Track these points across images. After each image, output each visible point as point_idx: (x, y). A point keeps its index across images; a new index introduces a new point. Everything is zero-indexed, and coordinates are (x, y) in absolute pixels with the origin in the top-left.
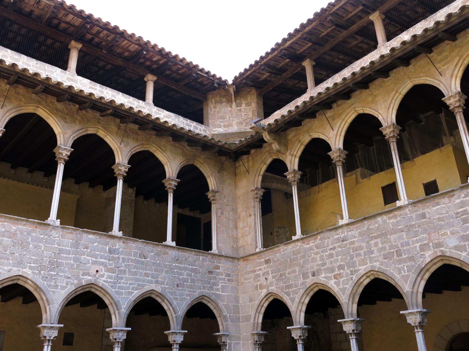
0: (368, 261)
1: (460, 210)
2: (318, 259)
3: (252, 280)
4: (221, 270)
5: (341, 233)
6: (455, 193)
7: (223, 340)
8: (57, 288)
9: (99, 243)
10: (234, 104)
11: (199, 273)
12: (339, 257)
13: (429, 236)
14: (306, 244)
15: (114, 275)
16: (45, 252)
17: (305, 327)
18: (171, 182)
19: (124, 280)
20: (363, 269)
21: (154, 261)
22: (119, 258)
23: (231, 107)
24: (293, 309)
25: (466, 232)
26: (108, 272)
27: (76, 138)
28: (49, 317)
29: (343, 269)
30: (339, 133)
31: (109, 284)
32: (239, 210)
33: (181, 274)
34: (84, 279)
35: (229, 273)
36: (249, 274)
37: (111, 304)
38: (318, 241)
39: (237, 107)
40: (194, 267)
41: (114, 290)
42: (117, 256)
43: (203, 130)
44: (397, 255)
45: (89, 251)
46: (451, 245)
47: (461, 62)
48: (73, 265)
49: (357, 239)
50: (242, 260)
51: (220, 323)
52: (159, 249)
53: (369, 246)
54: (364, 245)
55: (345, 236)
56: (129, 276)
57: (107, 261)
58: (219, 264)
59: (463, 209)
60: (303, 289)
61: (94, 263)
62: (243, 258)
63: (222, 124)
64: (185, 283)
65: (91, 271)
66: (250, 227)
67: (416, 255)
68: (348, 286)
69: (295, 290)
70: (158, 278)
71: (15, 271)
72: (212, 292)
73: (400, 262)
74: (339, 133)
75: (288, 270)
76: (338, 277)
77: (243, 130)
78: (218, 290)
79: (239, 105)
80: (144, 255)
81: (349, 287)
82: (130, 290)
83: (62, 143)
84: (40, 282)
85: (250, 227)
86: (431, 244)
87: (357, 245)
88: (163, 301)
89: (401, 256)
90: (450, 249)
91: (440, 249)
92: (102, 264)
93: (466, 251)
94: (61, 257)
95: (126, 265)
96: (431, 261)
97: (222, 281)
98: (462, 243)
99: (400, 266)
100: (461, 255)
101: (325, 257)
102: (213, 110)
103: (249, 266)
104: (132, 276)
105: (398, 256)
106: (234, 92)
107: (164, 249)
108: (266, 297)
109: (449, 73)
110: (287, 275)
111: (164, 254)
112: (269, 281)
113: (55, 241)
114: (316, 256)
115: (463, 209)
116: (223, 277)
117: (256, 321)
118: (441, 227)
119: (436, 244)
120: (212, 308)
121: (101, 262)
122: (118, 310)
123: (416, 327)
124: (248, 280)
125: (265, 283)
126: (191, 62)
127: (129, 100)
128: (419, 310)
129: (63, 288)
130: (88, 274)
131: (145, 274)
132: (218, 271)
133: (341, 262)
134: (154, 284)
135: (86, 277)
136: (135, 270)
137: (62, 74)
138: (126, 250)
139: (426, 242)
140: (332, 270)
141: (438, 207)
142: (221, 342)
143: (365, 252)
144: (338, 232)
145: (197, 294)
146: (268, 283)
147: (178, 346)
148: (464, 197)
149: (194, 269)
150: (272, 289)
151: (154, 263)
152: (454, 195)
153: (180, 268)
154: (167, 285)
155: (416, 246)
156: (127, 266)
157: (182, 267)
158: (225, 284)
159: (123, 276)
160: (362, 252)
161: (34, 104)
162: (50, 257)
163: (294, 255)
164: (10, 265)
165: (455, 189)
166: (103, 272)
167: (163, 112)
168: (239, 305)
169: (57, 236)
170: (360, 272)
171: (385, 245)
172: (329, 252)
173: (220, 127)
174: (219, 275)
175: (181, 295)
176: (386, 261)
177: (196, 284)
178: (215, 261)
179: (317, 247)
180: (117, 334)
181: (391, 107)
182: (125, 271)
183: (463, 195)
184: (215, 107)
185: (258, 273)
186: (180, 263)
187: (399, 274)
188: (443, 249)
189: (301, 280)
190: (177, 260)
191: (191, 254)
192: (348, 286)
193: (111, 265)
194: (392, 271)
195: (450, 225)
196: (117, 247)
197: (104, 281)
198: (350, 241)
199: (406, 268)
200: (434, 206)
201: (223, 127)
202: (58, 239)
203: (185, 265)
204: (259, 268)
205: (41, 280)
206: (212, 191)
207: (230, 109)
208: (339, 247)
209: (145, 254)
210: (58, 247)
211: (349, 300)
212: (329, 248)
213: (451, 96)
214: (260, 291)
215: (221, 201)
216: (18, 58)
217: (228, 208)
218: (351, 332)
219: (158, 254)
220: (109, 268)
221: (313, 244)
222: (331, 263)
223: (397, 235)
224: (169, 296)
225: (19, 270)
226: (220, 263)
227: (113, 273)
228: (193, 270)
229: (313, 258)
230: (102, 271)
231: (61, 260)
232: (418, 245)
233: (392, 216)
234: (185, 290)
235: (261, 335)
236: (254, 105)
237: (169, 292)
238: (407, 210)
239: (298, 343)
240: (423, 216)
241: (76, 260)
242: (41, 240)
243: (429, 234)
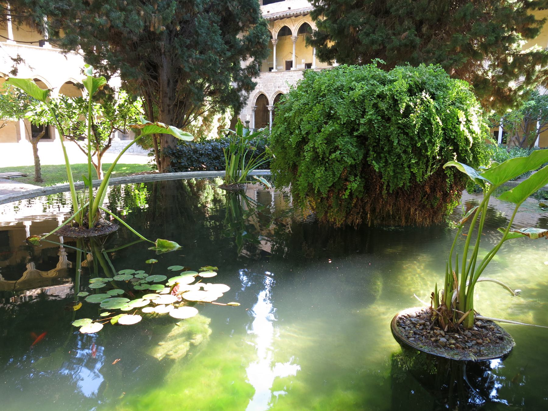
38: (282, 75)
112: (260, 87)
179: (281, 77)
189: (274, 89)
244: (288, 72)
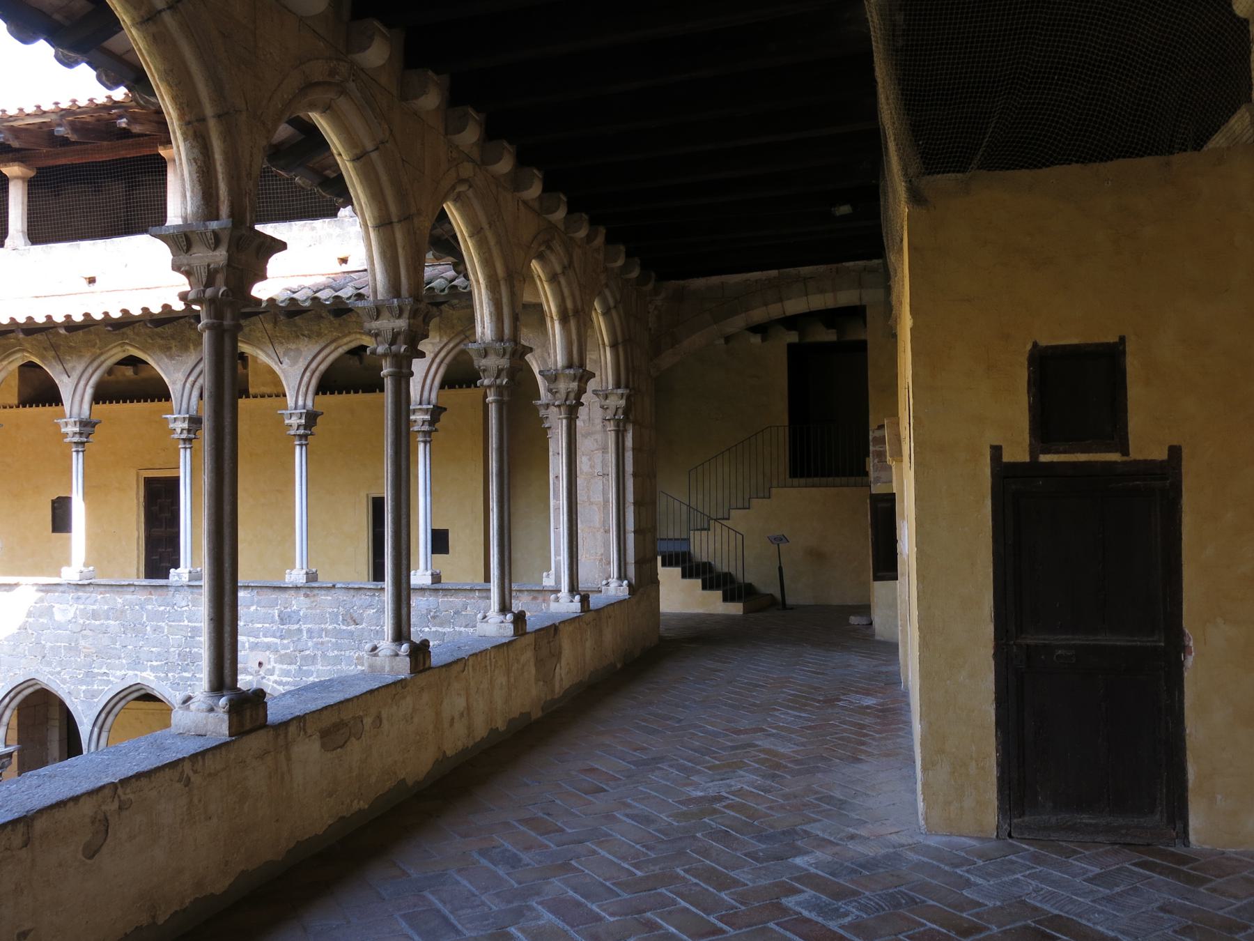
9: (258, 604)
15: (293, 667)
21: (378, 628)
22: (300, 630)
26: (282, 663)
42: (296, 627)
56: (324, 668)
57: (278, 641)
65: (249, 665)
80: (352, 618)
92: (268, 647)
95: (317, 644)
104: (329, 667)
113: (182, 613)
121: (267, 643)
136: (336, 652)
138: (314, 612)
151: (377, 631)
156: (319, 646)
157: (449, 632)
159: (310, 668)
161: (115, 341)
162: (179, 646)
164: (121, 668)
169: (184, 603)
186: (441, 625)
190: (434, 617)
191: (470, 598)
196: (295, 607)
197: (275, 682)
202: (187, 608)
203: (457, 629)
205: (170, 689)
209: (355, 616)
210: (190, 624)
220: (283, 655)
225: (136, 675)
227: (290, 664)
230: (269, 662)
231: (196, 650)
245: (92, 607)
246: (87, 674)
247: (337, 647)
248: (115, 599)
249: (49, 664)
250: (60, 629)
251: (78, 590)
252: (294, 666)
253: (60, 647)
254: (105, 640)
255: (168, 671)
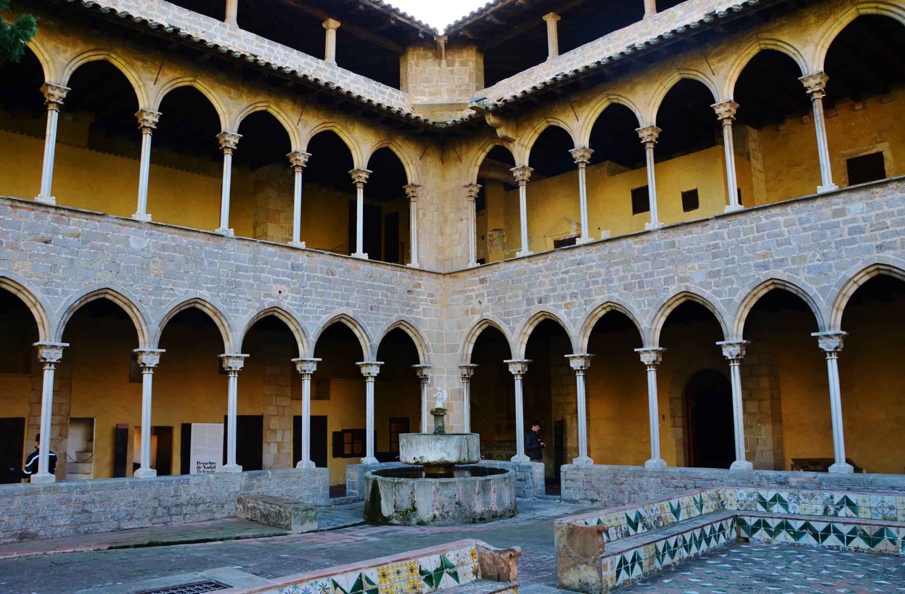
0: (606, 291)
1: (711, 243)
2: (547, 283)
3: (462, 302)
4: (422, 289)
5: (577, 255)
6: (710, 222)
7: (424, 373)
8: (238, 313)
9: (279, 257)
10: (444, 62)
11: (397, 293)
12: (573, 283)
13: (676, 268)
14: (534, 264)
15: (298, 296)
16: (221, 270)
17: (526, 360)
18: (360, 175)
19: (311, 301)
20: (599, 299)
22: (303, 275)
23: (439, 65)
24: (513, 340)
25: (713, 268)
26: (292, 293)
27: (243, 118)
28: (232, 346)
29: (576, 297)
30: (585, 125)
31: (295, 307)
32: (447, 210)
33: (375, 294)
34: (266, 301)
35: (432, 292)
36: (458, 294)
37: (297, 330)
38: (548, 262)
39: (448, 66)
40: (390, 286)
41: (300, 314)
42: (301, 273)
43: (401, 98)
44: (639, 286)
45: (269, 267)
46: (697, 281)
47: (738, 62)
48: (253, 285)
49: (595, 263)
50: (448, 276)
51: (420, 353)
52: (349, 263)
53: (608, 273)
54: (603, 271)
55: (581, 259)
58: (420, 282)
59: (714, 242)
60: (526, 317)
61: (276, 282)
62: (450, 274)
63: (427, 90)
64: (380, 306)
65: (272, 292)
66: (460, 235)
67: (659, 288)
68: (581, 317)
69: (516, 318)
70: (349, 299)
71: (192, 294)
72: (412, 316)
73: (641, 294)
74: (585, 125)
75: (509, 294)
76: (569, 306)
77: (455, 101)
78: (418, 313)
79: (450, 64)
80: (331, 272)
81: (581, 318)
82: (318, 315)
83: (228, 127)
84: (221, 307)
85: (460, 235)
86: (676, 278)
87: (594, 270)
88: (355, 326)
89: (643, 288)
90: (695, 285)
91: (685, 284)
92: (285, 283)
93: (710, 288)
94: (240, 275)
95: (312, 284)
96: (675, 296)
97: (423, 303)
98: (708, 280)
99: (640, 299)
100: (706, 293)
101: (556, 282)
102: (414, 69)
103: (457, 285)
105: (640, 288)
106: (446, 45)
107: (355, 263)
108: (479, 324)
109: (722, 73)
110: (508, 300)
111: (355, 269)
112: (484, 305)
113: (230, 255)
114: (544, 279)
115: (714, 242)
116: (425, 297)
117: (465, 352)
118: (689, 260)
119: (681, 278)
120: (411, 335)
122: (306, 337)
123: (650, 365)
124: (456, 301)
125: (478, 307)
126: (390, 5)
127: (305, 60)
128: (655, 348)
129: (245, 312)
130: (270, 296)
131: (334, 294)
132: (419, 290)
133: (575, 289)
134: (345, 307)
135: (268, 299)
137: (222, 28)
138: (311, 265)
139: (672, 275)
140: (563, 297)
141: (690, 236)
142: (422, 375)
143: (603, 280)
144: (574, 253)
145: (394, 319)
146: (483, 308)
147: (373, 379)
148: (718, 229)
149: (391, 287)
150: (486, 315)
152: (708, 225)
153: (373, 287)
154: (359, 308)
155: (661, 279)
158: (427, 307)
160: (600, 279)
163: (517, 275)
164: (185, 286)
165: (709, 218)
166: (287, 292)
167: (349, 75)
168: (444, 331)
170: (596, 302)
171: (627, 274)
172: (561, 276)
173: (424, 94)
174: (419, 295)
175: (376, 320)
176: (626, 292)
177: (393, 306)
178: (416, 277)
179: (547, 269)
180: (306, 365)
181: (653, 103)
182: (311, 291)
183: (717, 226)
184: (417, 65)
185: (469, 294)
186: (373, 281)
187: (638, 308)
188: (688, 284)
189: (524, 307)
190: (371, 276)
191: (387, 269)
192: (581, 317)
193: (294, 284)
194: (631, 304)
195: (699, 258)
197: (288, 304)
198: (588, 265)
199: (646, 302)
200: (686, 235)
201: (427, 95)
202: (234, 253)
204: (471, 288)
205: (220, 303)
206: (412, 185)
207: (438, 68)
208: (574, 271)
211: (580, 333)
212: (562, 271)
213: (721, 104)
214: (472, 316)
215: (423, 199)
216: (166, 9)
217: (432, 208)
218: (579, 368)
219: (348, 270)
221: (541, 265)
222: (563, 289)
223: (642, 263)
224: (362, 321)
225: (196, 292)
226: (421, 280)
227: (298, 294)
228: (388, 289)
229: (541, 282)
232: (662, 277)
233: (639, 241)
234: (380, 314)
235: (471, 368)
236: (471, 65)
237: (362, 316)
238: (656, 235)
239: (515, 378)
240: (673, 245)
241: (256, 278)
242: (215, 255)
243: (676, 266)
244: (567, 253)
245: (163, 242)
246: (156, 288)
247: (323, 287)
248: (182, 240)
249: (123, 278)
250: (133, 254)
251: (152, 229)
252: (299, 295)
253: (134, 267)
254: (171, 266)
255: (219, 291)
